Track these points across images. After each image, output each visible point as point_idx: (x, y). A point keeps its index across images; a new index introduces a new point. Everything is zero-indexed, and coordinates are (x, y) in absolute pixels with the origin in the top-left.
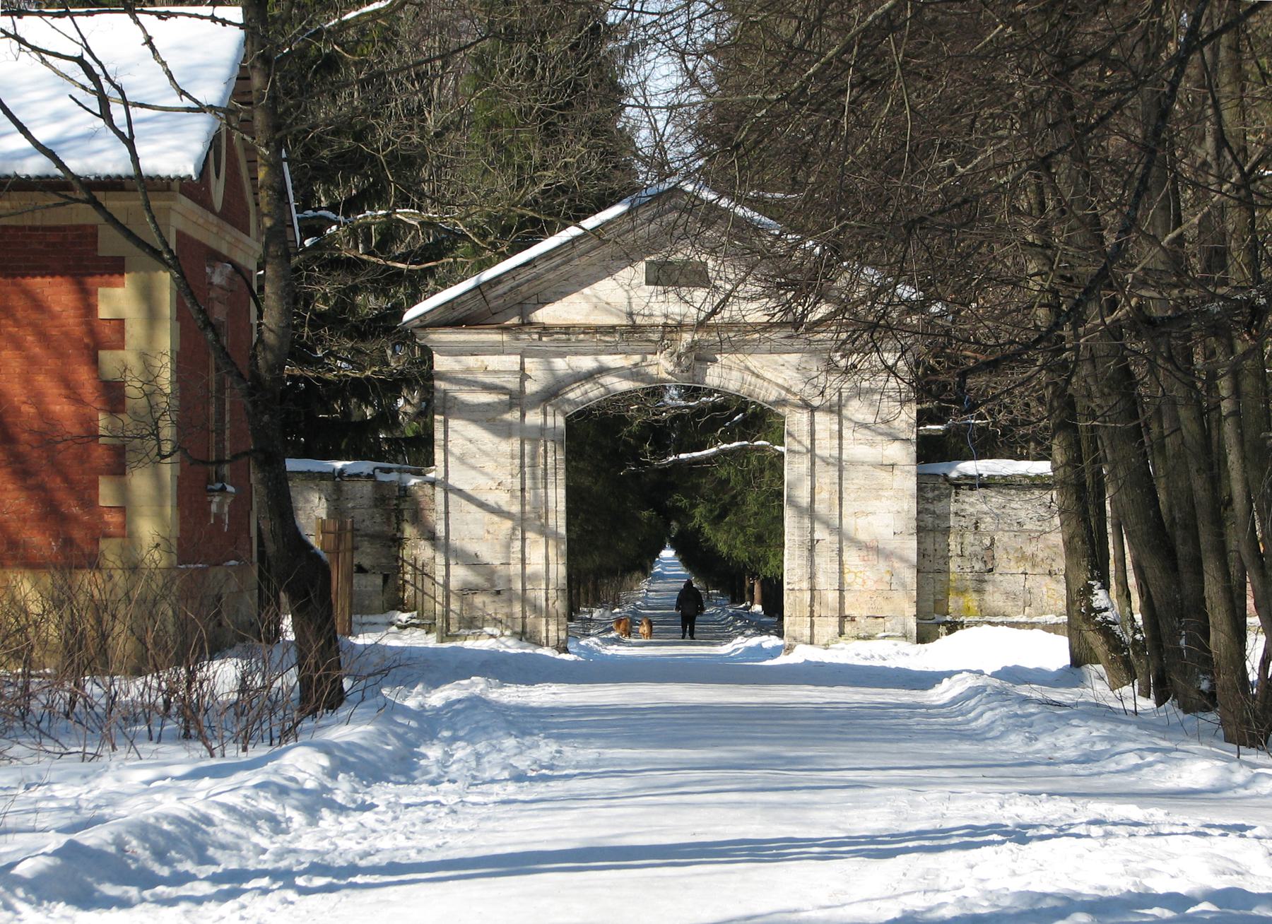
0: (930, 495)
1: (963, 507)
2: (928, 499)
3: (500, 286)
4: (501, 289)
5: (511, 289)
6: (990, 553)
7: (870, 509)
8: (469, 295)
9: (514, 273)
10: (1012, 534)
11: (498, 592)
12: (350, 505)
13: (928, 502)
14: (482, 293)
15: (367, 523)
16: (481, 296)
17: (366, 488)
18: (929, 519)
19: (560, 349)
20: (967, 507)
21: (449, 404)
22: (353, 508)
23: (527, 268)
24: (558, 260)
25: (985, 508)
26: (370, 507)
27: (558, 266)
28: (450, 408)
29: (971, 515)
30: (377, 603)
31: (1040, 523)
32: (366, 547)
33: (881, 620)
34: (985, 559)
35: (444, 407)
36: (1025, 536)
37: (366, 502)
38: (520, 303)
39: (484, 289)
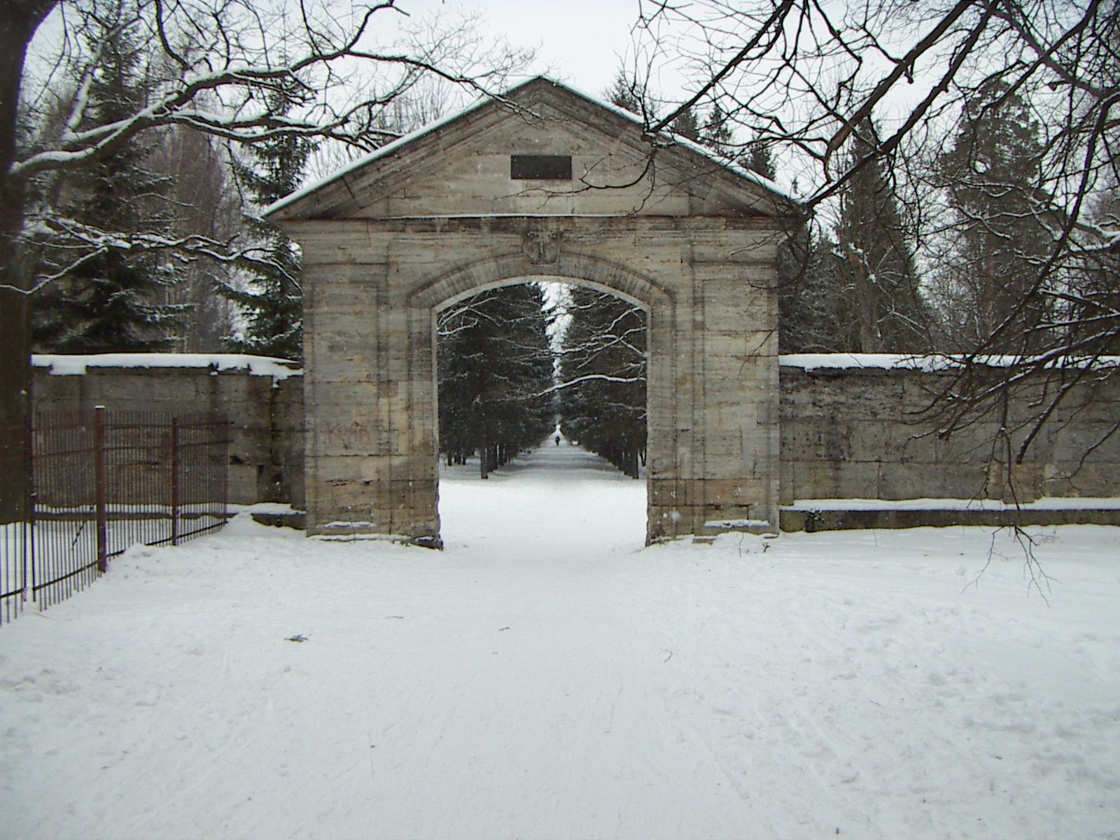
0: (790, 385)
1: (819, 398)
2: (787, 389)
3: (365, 178)
4: (366, 181)
5: (376, 182)
6: (845, 442)
7: (735, 399)
8: (333, 186)
9: (380, 164)
10: (867, 423)
11: (367, 483)
12: (225, 399)
13: (788, 393)
14: (346, 184)
15: (242, 415)
16: (345, 188)
17: (243, 384)
18: (789, 411)
19: (424, 242)
20: (824, 397)
21: (316, 299)
22: (228, 402)
23: (391, 159)
24: (422, 152)
25: (842, 399)
26: (245, 401)
27: (423, 158)
28: (318, 302)
29: (828, 405)
30: (253, 494)
31: (892, 413)
32: (240, 437)
33: (745, 508)
34: (842, 447)
35: (312, 301)
36: (879, 425)
37: (242, 395)
38: (388, 197)
39: (349, 179)
